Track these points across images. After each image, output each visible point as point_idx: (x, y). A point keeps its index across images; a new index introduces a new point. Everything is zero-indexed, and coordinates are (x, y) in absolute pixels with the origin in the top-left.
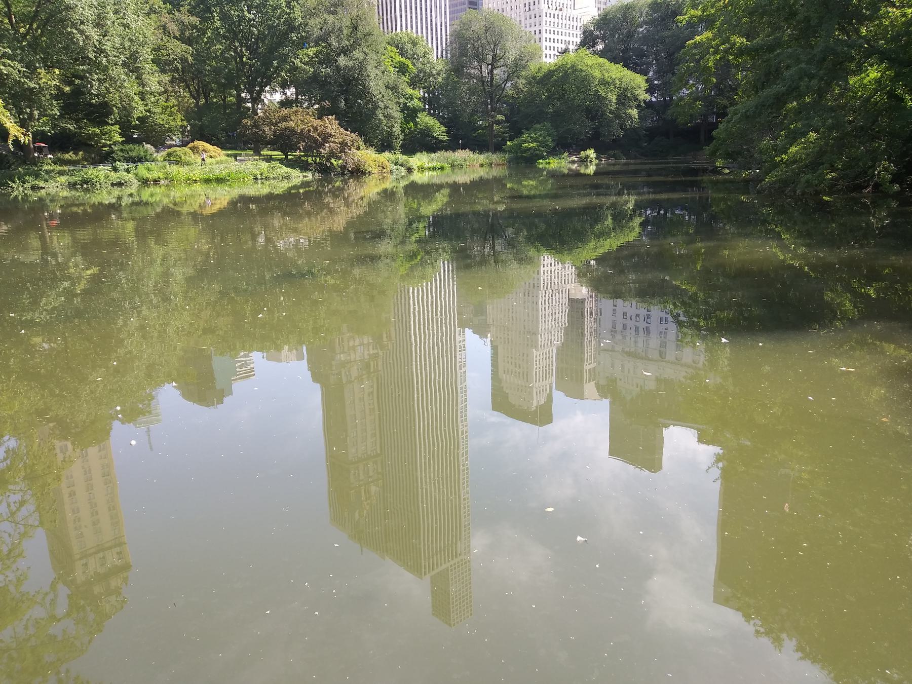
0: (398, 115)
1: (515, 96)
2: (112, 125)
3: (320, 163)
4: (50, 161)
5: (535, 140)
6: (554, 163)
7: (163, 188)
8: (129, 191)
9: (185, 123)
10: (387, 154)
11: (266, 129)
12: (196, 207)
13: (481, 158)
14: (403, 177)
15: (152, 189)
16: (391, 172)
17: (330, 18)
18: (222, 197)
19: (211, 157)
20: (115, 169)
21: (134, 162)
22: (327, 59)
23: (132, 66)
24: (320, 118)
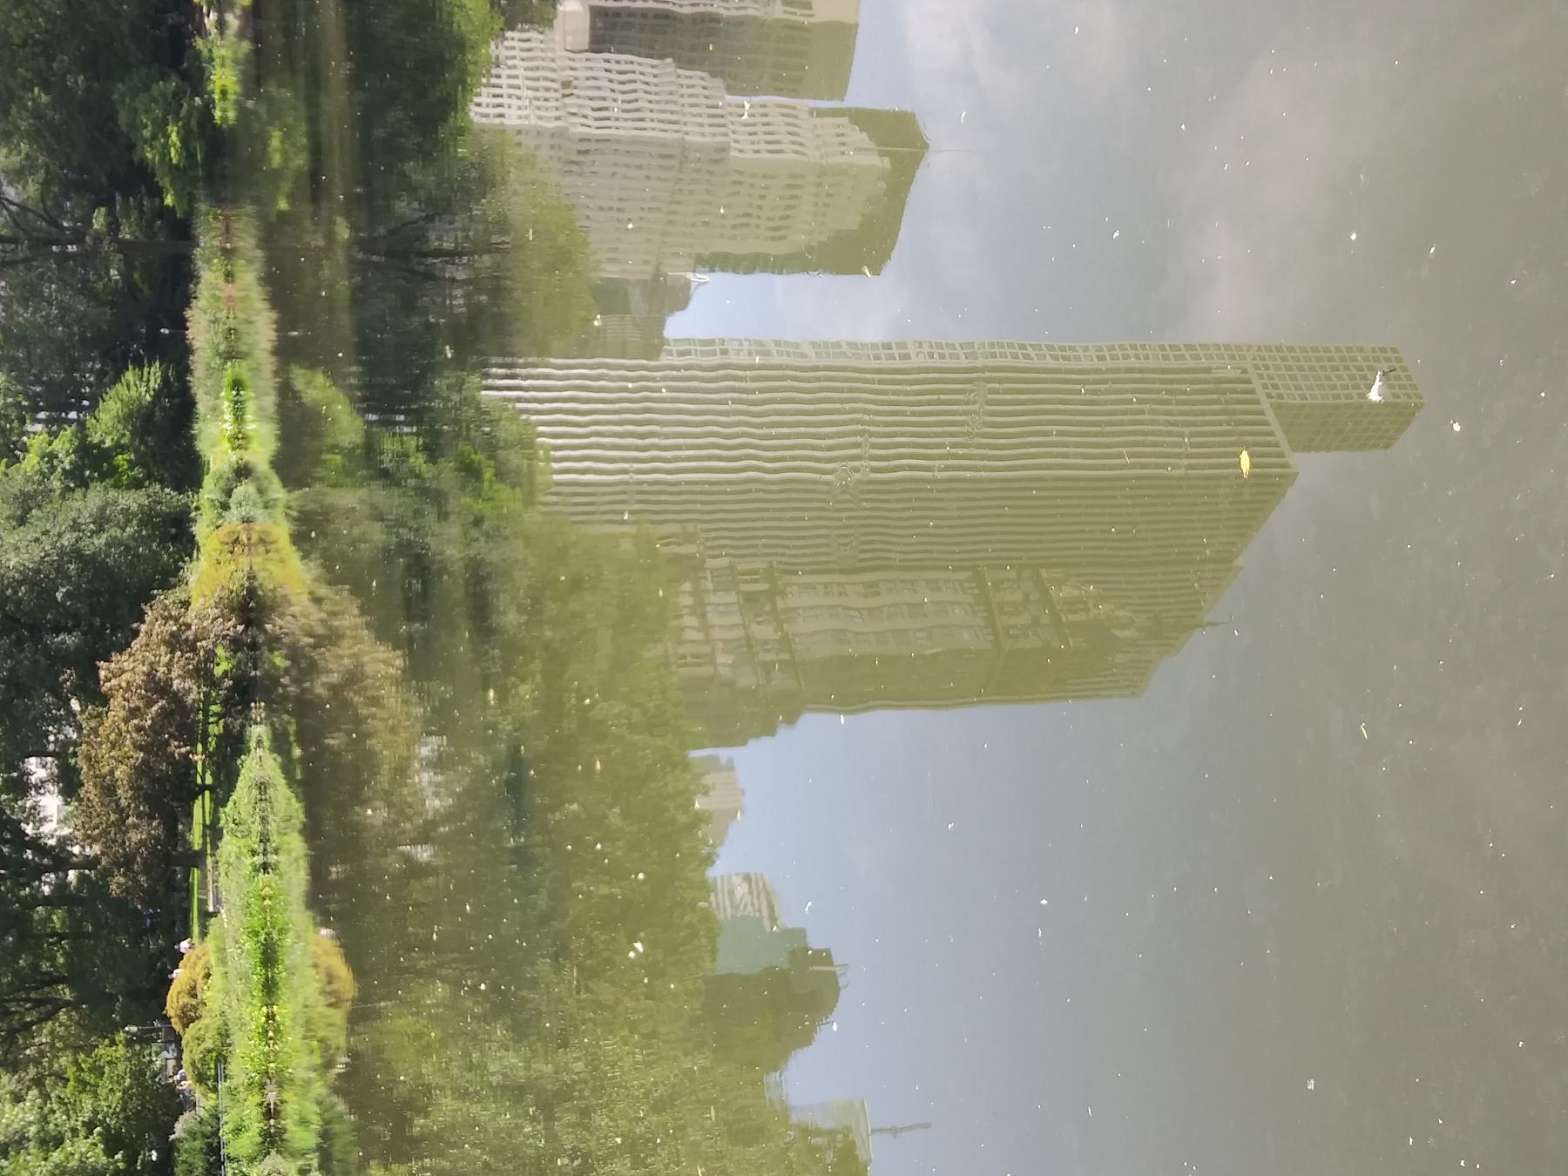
0: (95, 497)
3: (226, 702)
5: (160, 127)
6: (224, 79)
7: (285, 1096)
10: (201, 530)
11: (135, 837)
12: (338, 1016)
13: (209, 277)
14: (261, 491)
15: (289, 1123)
16: (247, 520)
18: (313, 949)
19: (208, 976)
24: (104, 700)
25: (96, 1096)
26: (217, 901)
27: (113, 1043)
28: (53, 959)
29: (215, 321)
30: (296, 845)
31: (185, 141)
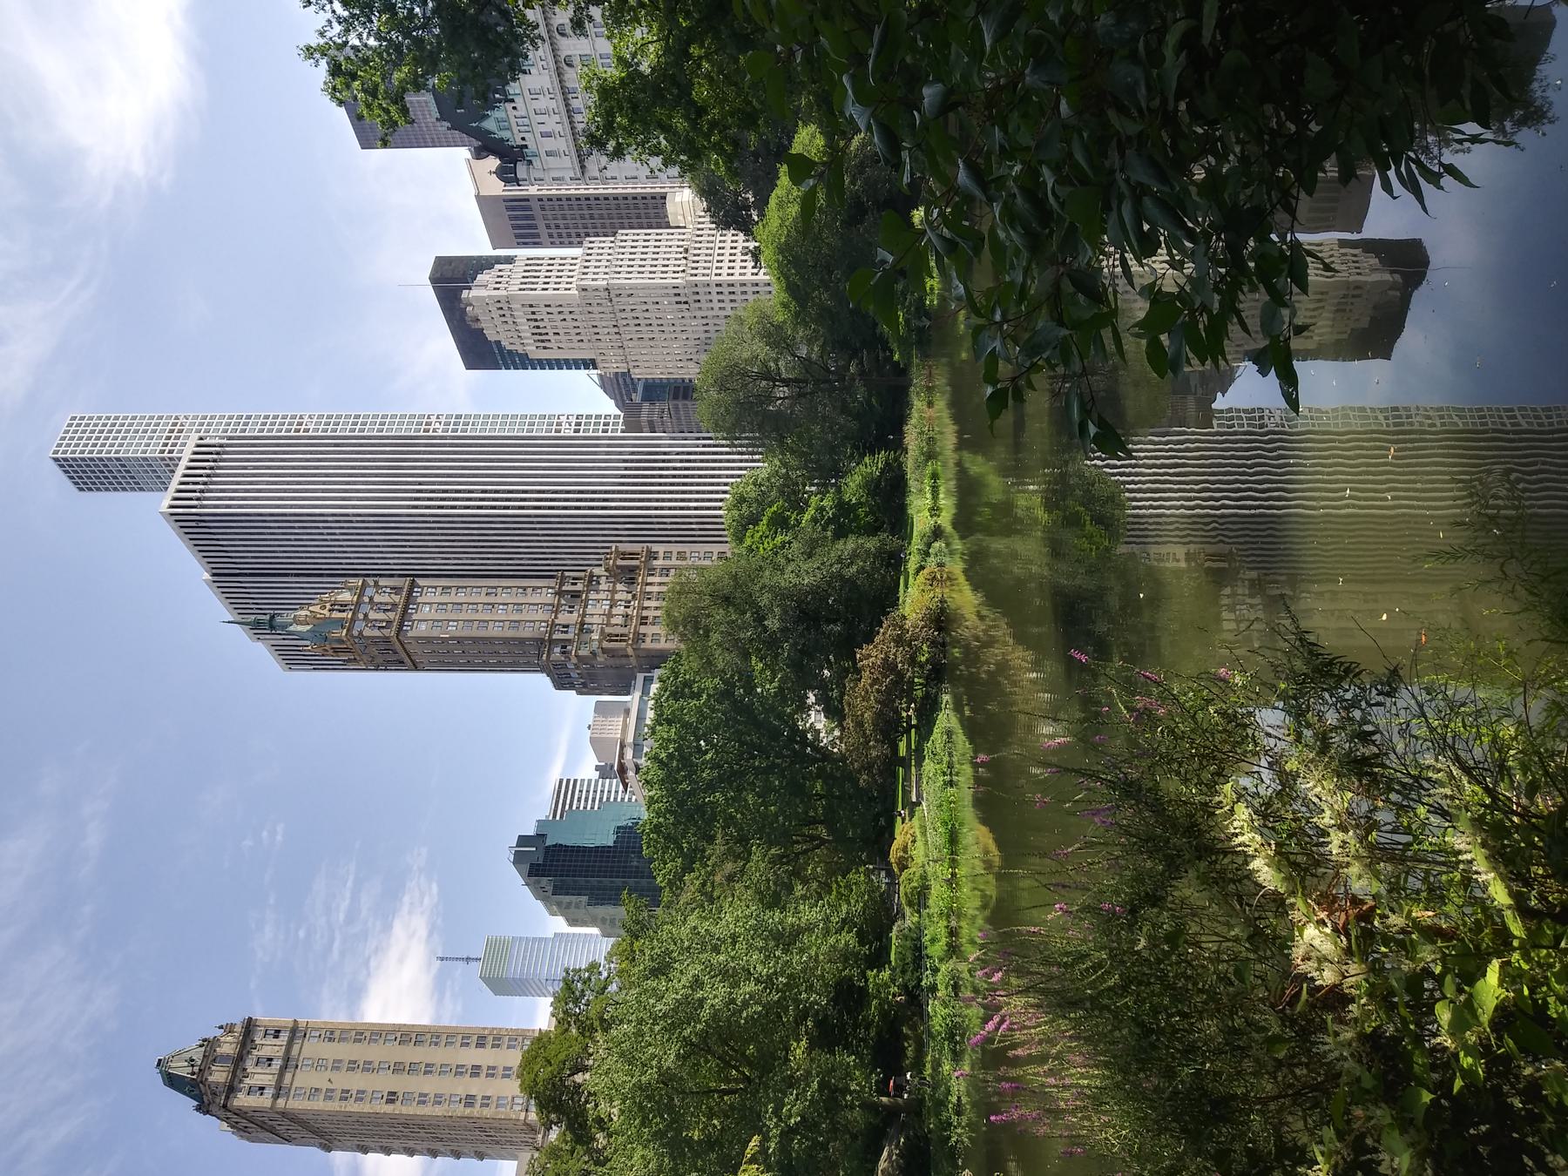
0: (849, 545)
1: (820, 342)
3: (927, 678)
7: (963, 924)
11: (874, 753)
13: (918, 404)
14: (948, 545)
16: (941, 565)
17: (715, 637)
18: (977, 837)
19: (914, 841)
20: (933, 988)
21: (920, 957)
22: (771, 643)
23: (787, 939)
24: (858, 671)
25: (849, 903)
26: (919, 796)
27: (858, 872)
28: (816, 810)
29: (922, 433)
30: (968, 769)
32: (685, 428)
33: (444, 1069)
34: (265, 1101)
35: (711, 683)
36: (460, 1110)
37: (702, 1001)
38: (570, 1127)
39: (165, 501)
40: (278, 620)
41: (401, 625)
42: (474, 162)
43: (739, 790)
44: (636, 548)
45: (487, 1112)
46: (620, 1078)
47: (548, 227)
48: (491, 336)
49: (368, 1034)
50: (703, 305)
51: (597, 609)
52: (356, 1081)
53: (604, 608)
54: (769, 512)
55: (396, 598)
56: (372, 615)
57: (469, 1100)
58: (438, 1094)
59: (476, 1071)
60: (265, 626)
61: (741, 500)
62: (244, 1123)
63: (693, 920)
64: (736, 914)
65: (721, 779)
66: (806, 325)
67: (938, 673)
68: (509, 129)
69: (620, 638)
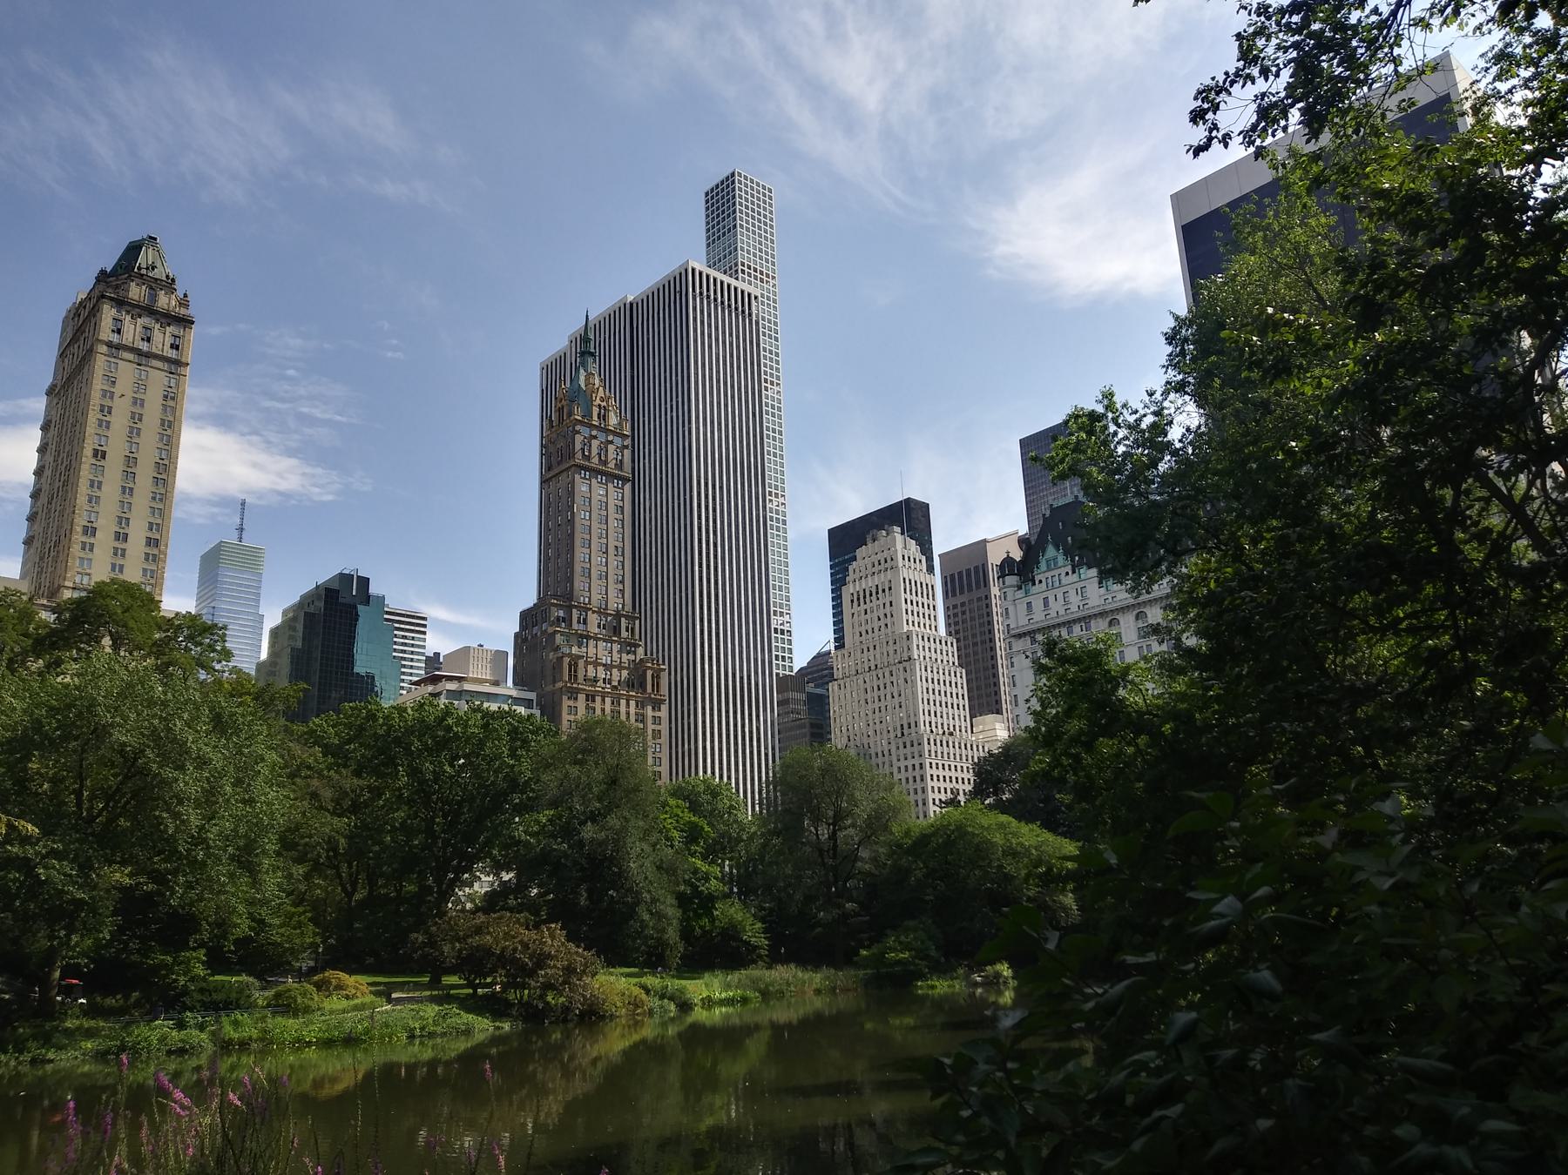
0: (672, 911)
1: (873, 871)
2: (194, 949)
3: (528, 1003)
4: (77, 1010)
5: (906, 947)
6: (941, 987)
8: (194, 1063)
9: (318, 940)
10: (651, 981)
11: (446, 949)
12: (306, 1086)
13: (817, 978)
14: (672, 1020)
16: (651, 1013)
17: (574, 771)
19: (347, 997)
20: (181, 1025)
23: (246, 860)
24: (537, 926)
25: (281, 926)
26: (399, 1001)
27: (315, 934)
29: (788, 984)
30: (428, 1054)
31: (899, 962)
32: (785, 733)
33: (125, 506)
34: (105, 333)
35: (526, 769)
36: (80, 521)
37: (181, 768)
38: (53, 632)
39: (699, 265)
40: (590, 360)
41: (586, 469)
42: (1015, 538)
43: (410, 802)
44: (664, 690)
45: (76, 549)
46: (105, 684)
47: (963, 604)
48: (861, 552)
49: (169, 432)
50: (902, 751)
51: (602, 651)
52: (120, 420)
53: (603, 658)
54: (703, 823)
55: (611, 465)
56: (595, 443)
57: (90, 531)
58: (100, 500)
59: (122, 537)
60: (584, 346)
61: (714, 793)
62: (84, 313)
63: (272, 756)
64: (276, 802)
65: (422, 782)
66: (890, 855)
67: (534, 1016)
68: (1049, 569)
69: (573, 675)
